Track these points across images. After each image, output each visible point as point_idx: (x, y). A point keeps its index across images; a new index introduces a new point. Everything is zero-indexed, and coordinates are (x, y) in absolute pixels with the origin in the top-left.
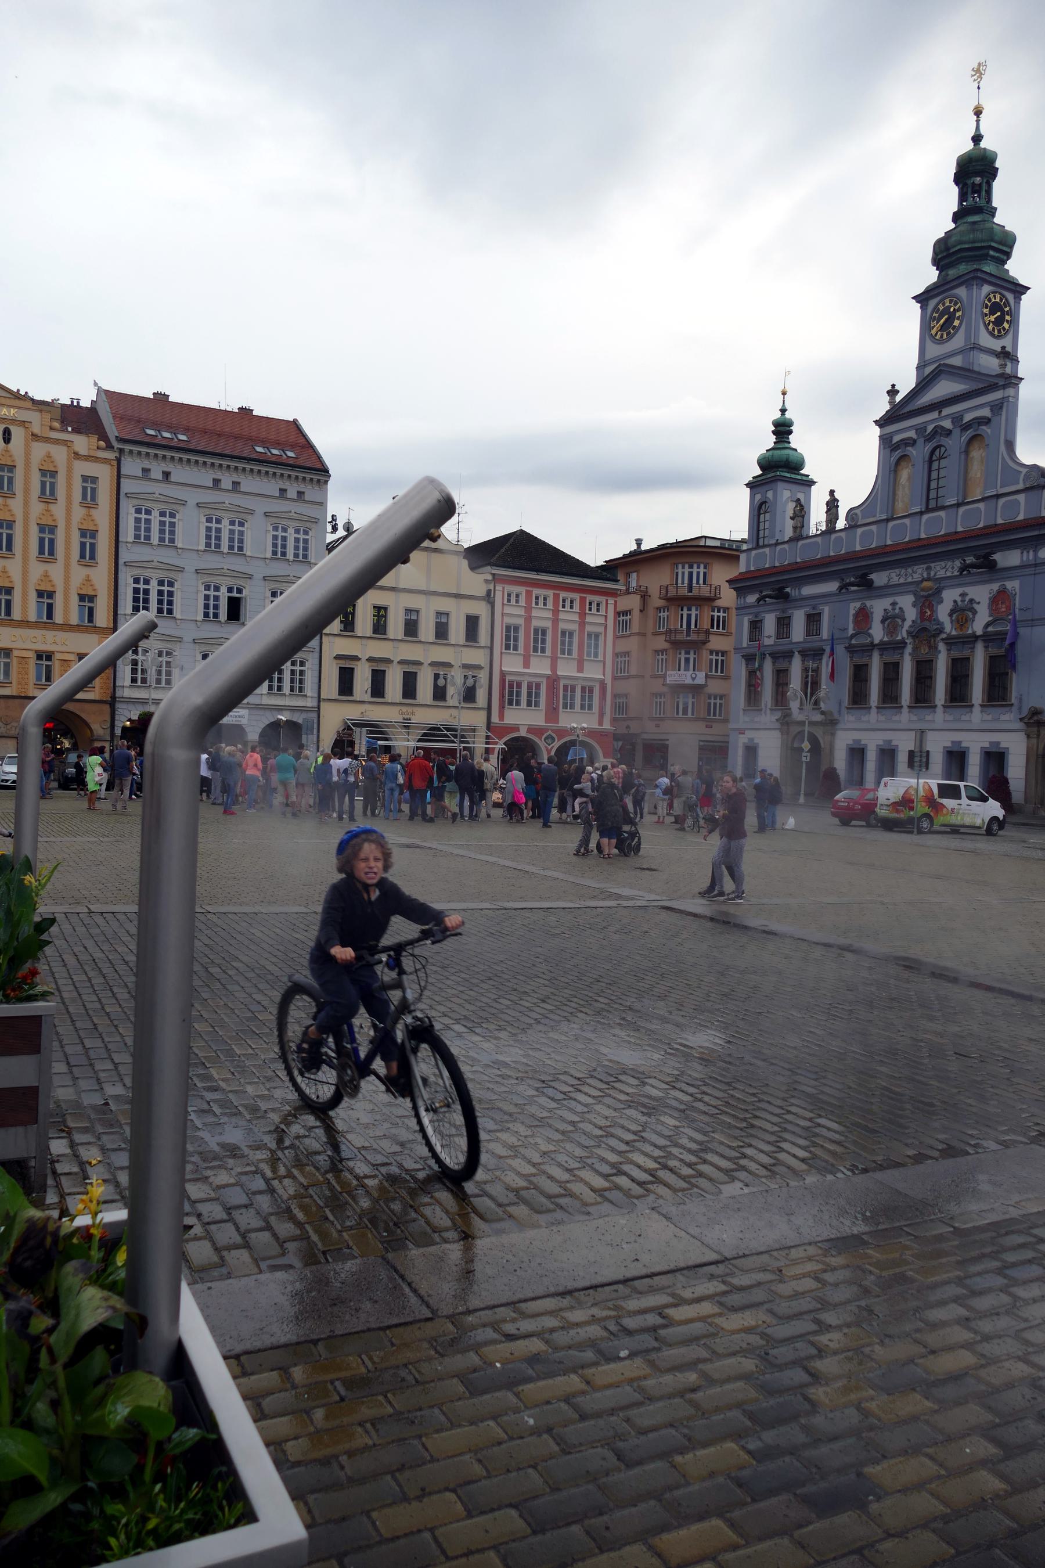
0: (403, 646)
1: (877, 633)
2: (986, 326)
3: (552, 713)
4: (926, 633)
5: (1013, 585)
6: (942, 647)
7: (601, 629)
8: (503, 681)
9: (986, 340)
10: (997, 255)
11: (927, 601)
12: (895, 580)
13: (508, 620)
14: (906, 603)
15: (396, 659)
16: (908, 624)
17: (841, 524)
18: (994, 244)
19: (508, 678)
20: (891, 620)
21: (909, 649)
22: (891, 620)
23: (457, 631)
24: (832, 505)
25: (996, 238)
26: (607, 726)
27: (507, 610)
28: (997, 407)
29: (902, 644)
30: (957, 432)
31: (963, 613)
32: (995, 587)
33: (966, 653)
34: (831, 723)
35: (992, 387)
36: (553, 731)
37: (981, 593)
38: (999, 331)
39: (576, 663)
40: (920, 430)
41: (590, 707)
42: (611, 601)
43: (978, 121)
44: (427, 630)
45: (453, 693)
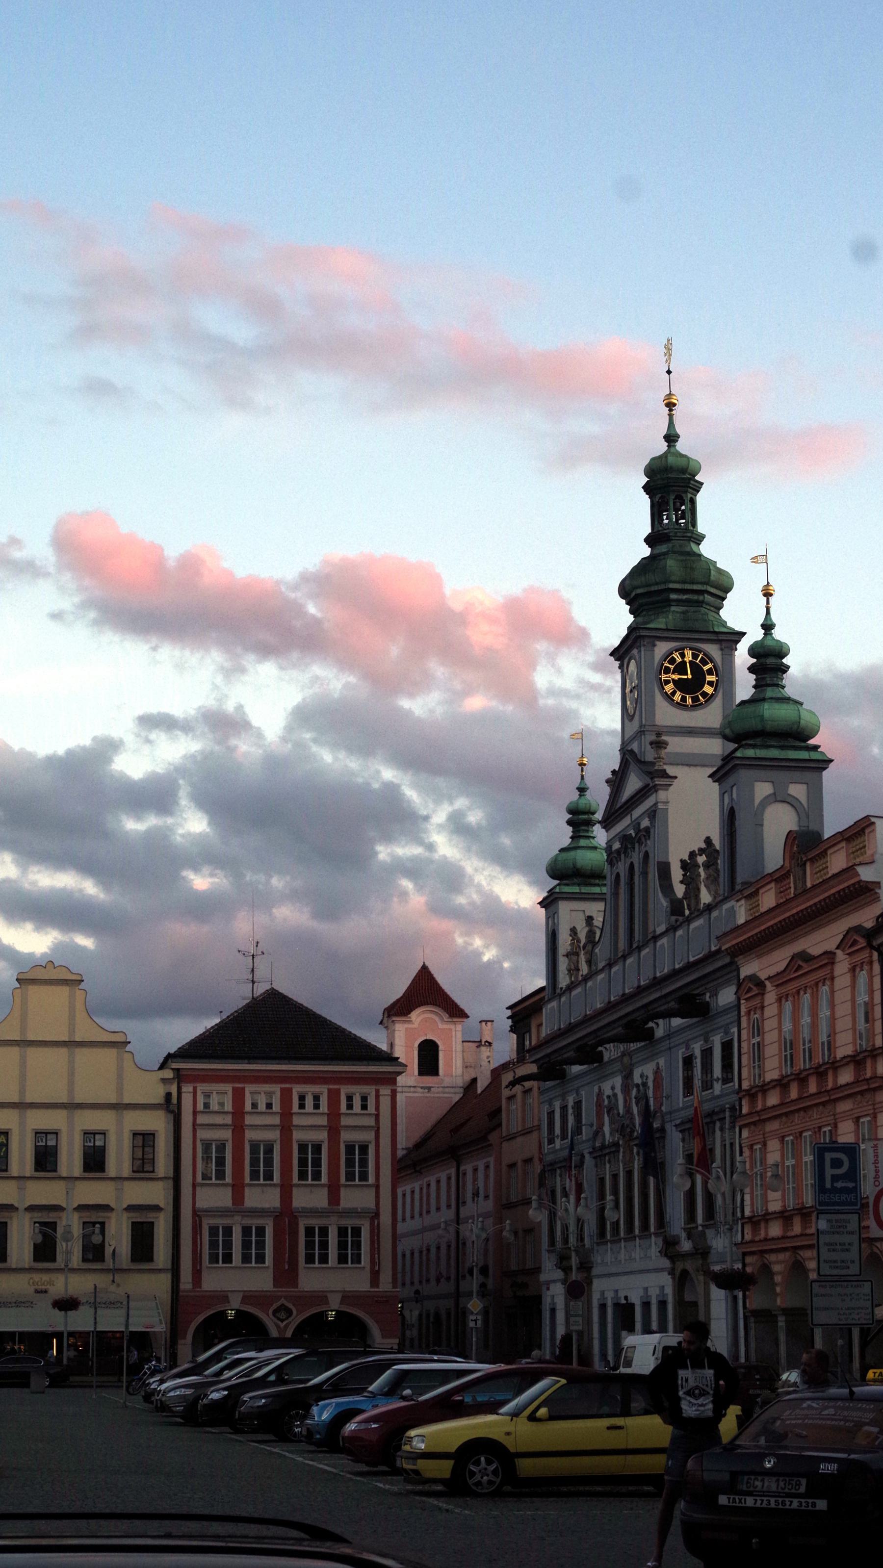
0: (31, 1185)
2: (669, 698)
3: (286, 1274)
5: (662, 1062)
7: (370, 1136)
8: (197, 1229)
9: (666, 715)
10: (685, 597)
13: (202, 1134)
15: (21, 1207)
18: (671, 586)
19: (206, 1223)
23: (119, 1159)
25: (673, 578)
26: (386, 1284)
27: (201, 1119)
28: (652, 814)
36: (286, 1297)
38: (695, 699)
39: (325, 1191)
41: (357, 1259)
42: (385, 1091)
43: (671, 416)
44: (70, 1160)
45: (70, 1250)
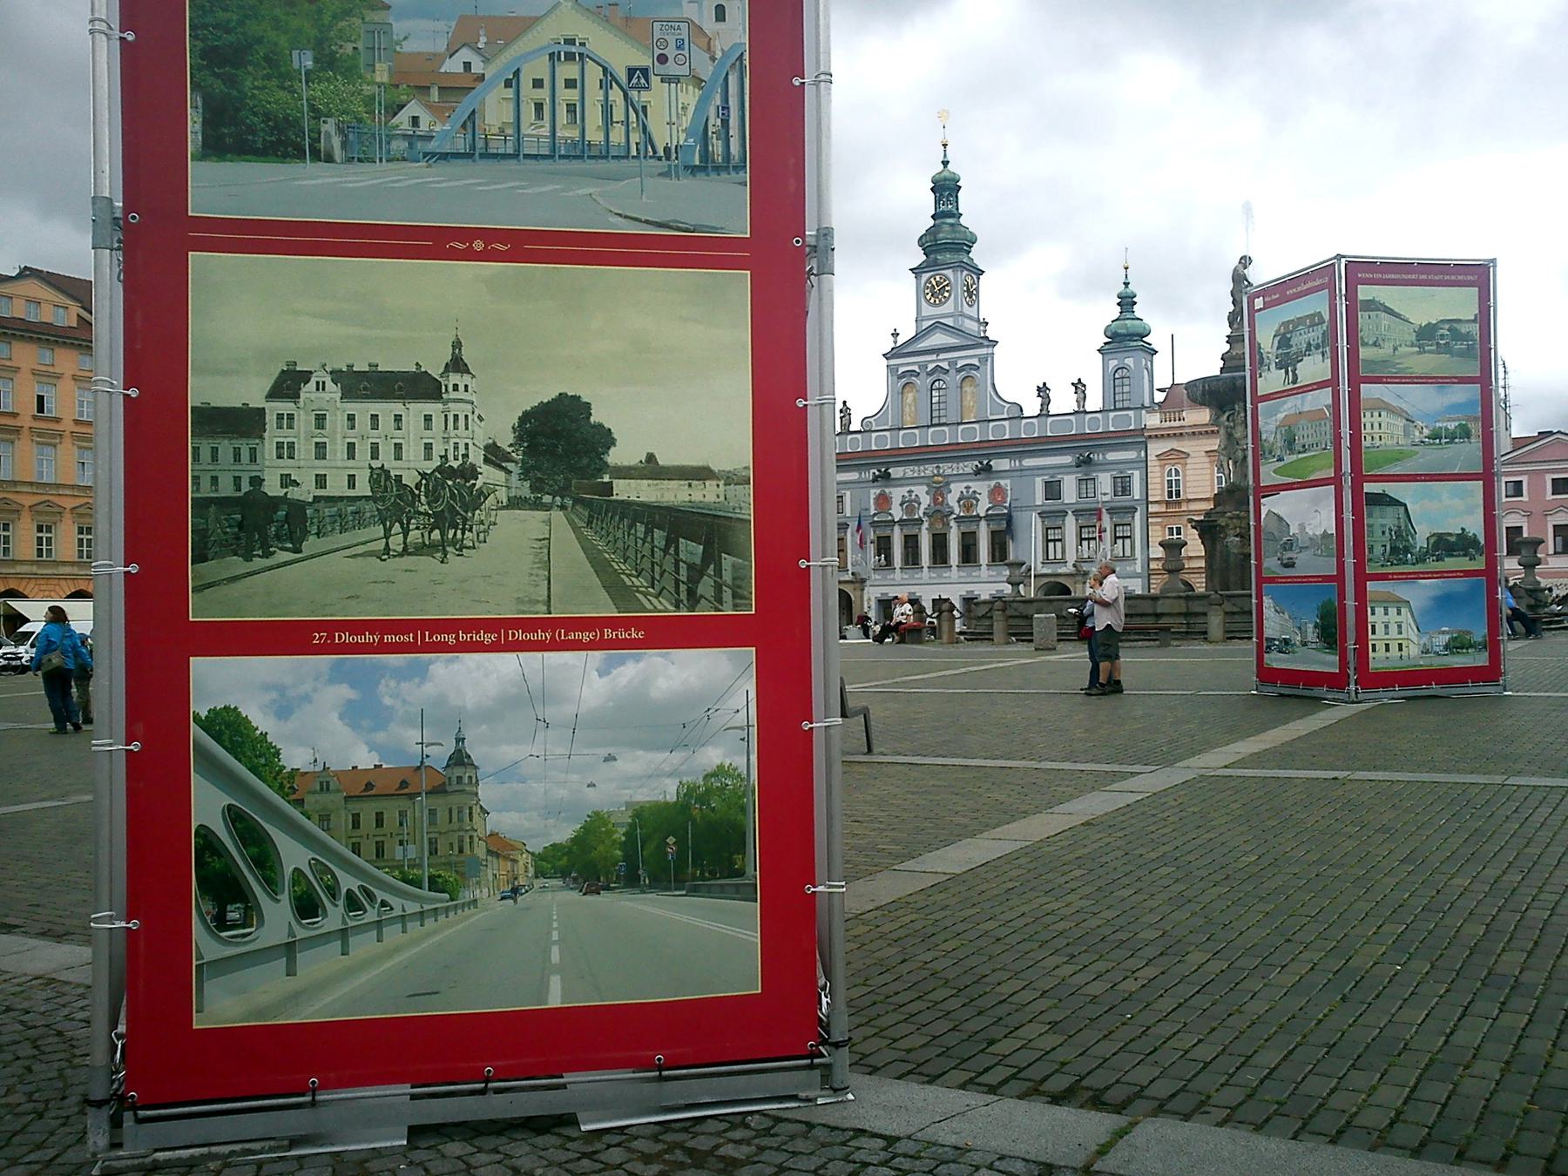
1: (897, 513)
4: (939, 513)
6: (952, 523)
11: (939, 490)
12: (909, 474)
14: (921, 491)
16: (923, 507)
17: (855, 426)
20: (909, 504)
21: (926, 525)
22: (909, 504)
24: (846, 411)
29: (920, 521)
30: (952, 372)
31: (968, 500)
32: (993, 483)
33: (973, 528)
34: (860, 582)
35: (981, 346)
37: (982, 487)
40: (923, 366)
